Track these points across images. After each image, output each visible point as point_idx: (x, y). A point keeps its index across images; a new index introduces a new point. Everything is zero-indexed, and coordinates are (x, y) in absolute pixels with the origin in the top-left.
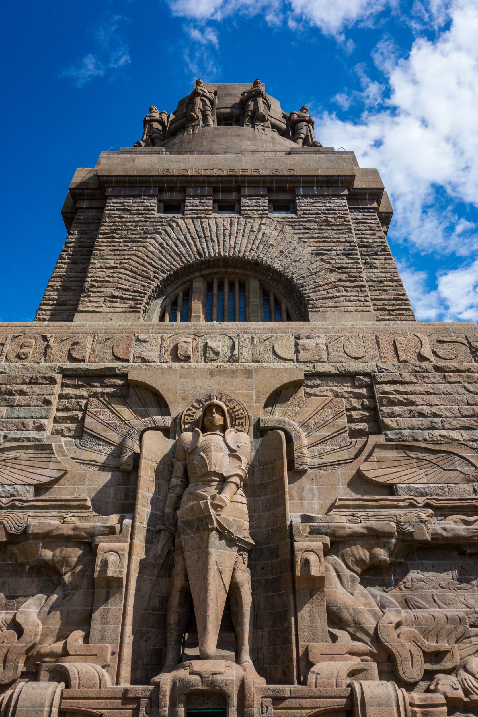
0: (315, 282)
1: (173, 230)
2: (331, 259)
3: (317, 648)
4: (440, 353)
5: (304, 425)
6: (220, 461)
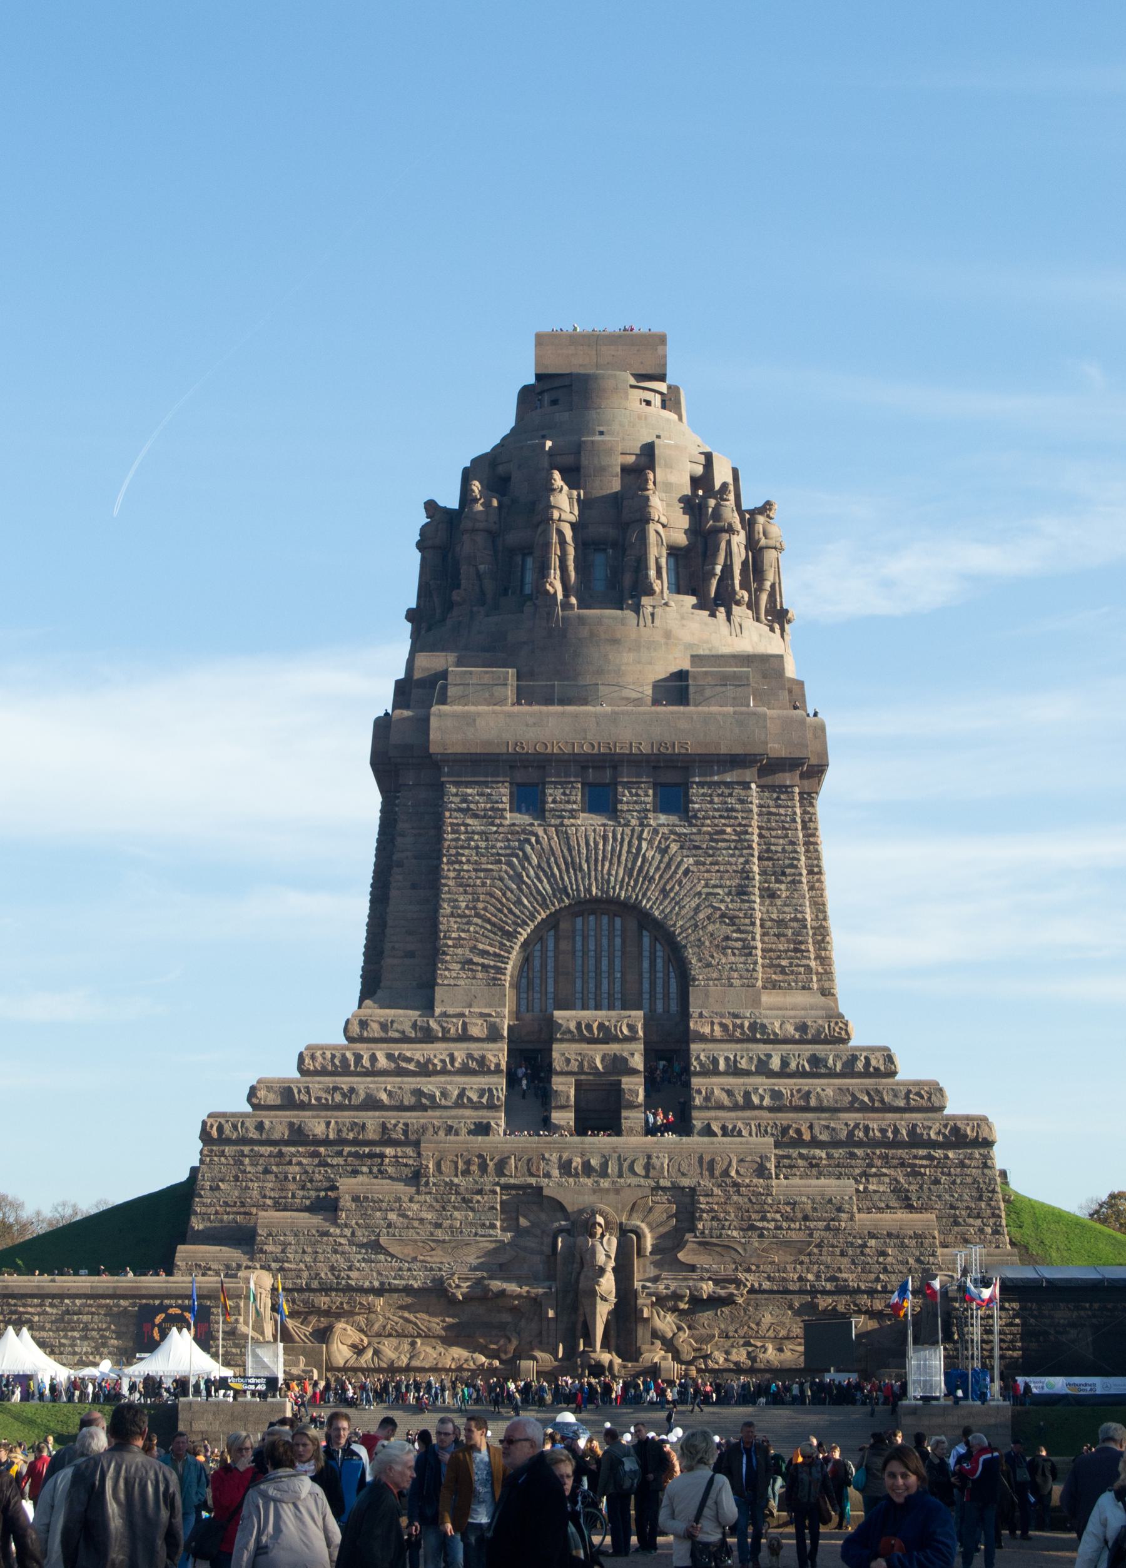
0: (699, 940)
1: (533, 849)
2: (722, 901)
3: (644, 1347)
4: (742, 1171)
5: (649, 1225)
6: (601, 1259)
